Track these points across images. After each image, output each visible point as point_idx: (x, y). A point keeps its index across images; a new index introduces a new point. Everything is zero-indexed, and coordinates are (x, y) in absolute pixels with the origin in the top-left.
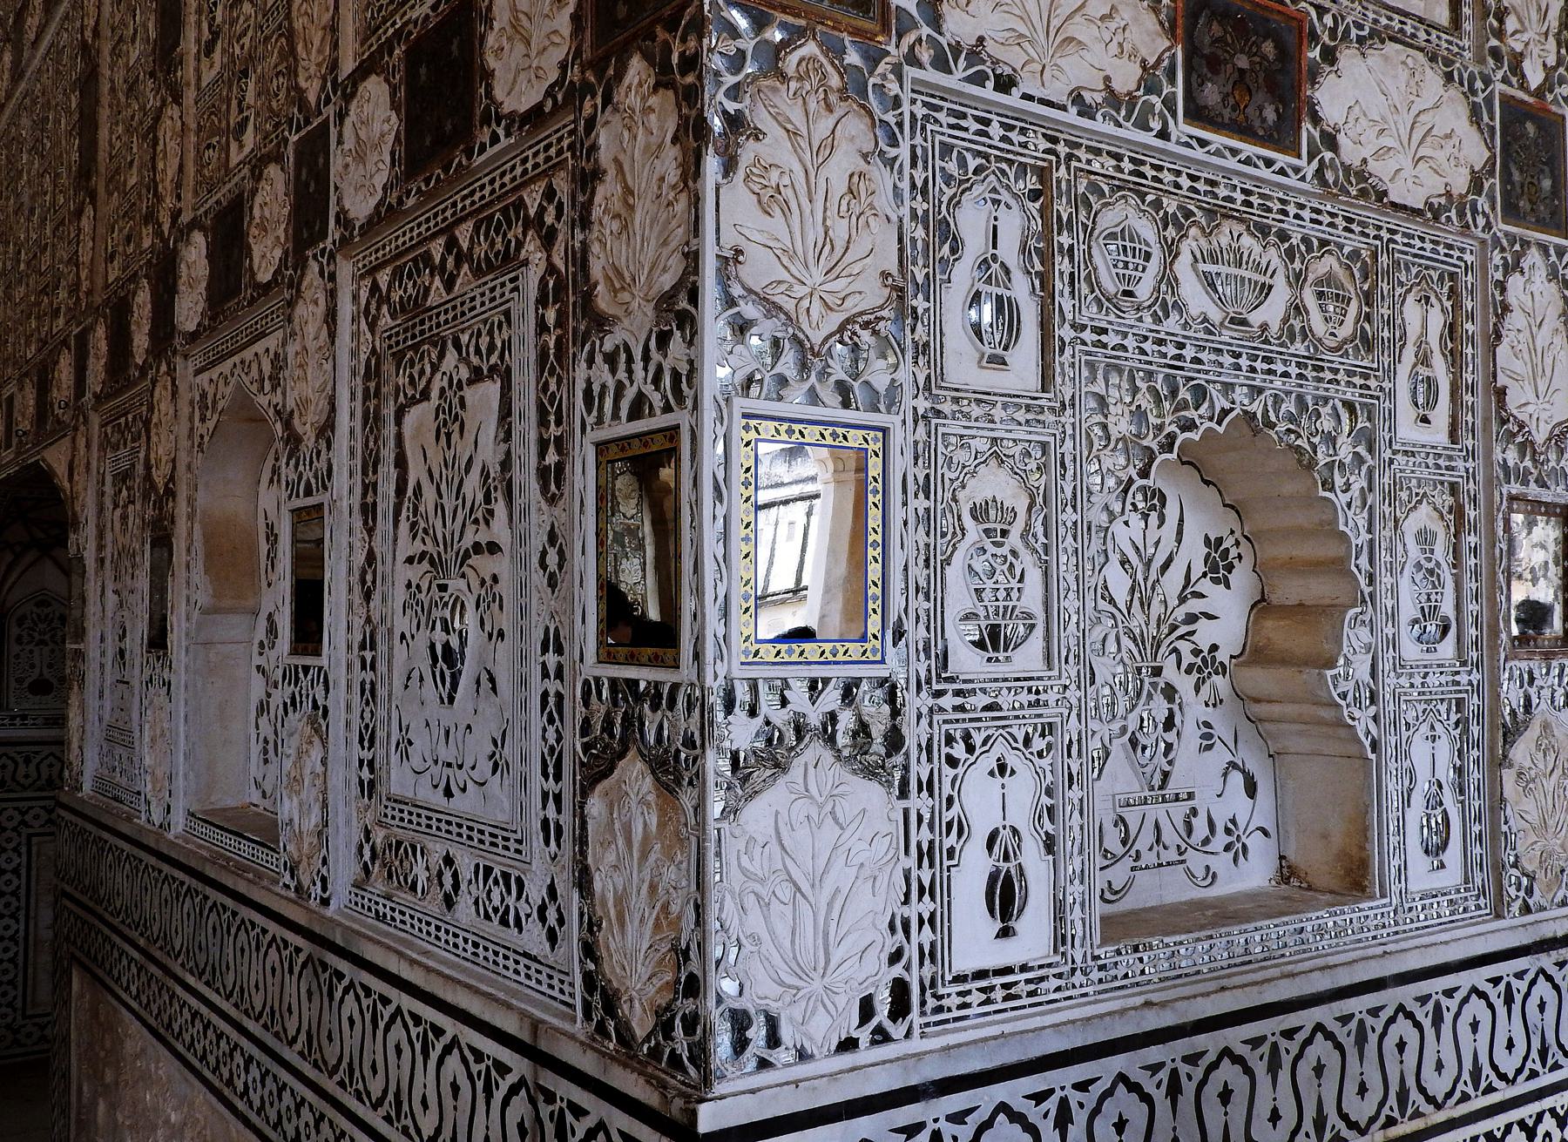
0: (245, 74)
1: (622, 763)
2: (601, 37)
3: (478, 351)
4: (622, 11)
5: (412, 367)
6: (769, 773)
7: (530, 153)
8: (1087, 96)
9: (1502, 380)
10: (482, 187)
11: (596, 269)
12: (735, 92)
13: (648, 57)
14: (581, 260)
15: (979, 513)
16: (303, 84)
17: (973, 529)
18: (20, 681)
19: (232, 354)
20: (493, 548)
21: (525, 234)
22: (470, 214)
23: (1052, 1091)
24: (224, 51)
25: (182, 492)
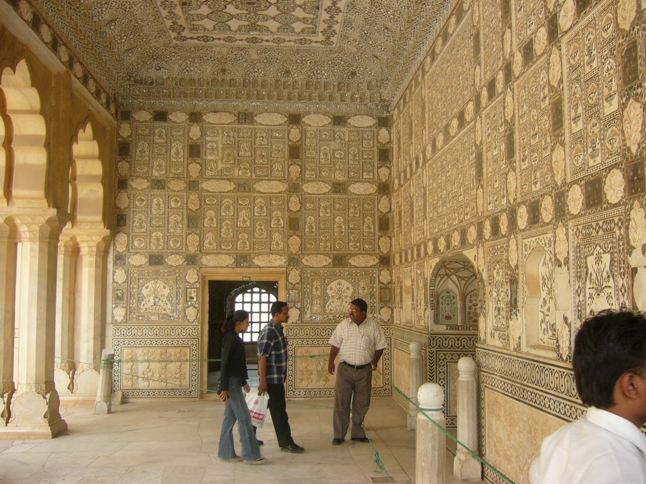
3: (605, 247)
4: (633, 191)
11: (631, 237)
13: (638, 201)
14: (628, 235)
18: (443, 316)
19: (535, 236)
20: (610, 287)
25: (520, 268)
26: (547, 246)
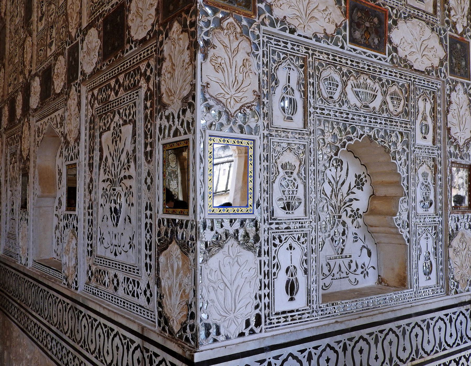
0: (52, 27)
1: (170, 245)
2: (165, 16)
3: (125, 115)
4: (171, 8)
5: (105, 120)
6: (217, 248)
7: (142, 52)
8: (318, 35)
9: (449, 125)
10: (127, 63)
11: (163, 89)
12: (207, 34)
13: (179, 22)
14: (158, 86)
15: (284, 167)
16: (70, 30)
17: (282, 172)
19: (48, 116)
20: (130, 177)
21: (140, 78)
22: (123, 72)
23: (306, 349)
24: (45, 20)
25: (32, 159)
26: (59, 126)
